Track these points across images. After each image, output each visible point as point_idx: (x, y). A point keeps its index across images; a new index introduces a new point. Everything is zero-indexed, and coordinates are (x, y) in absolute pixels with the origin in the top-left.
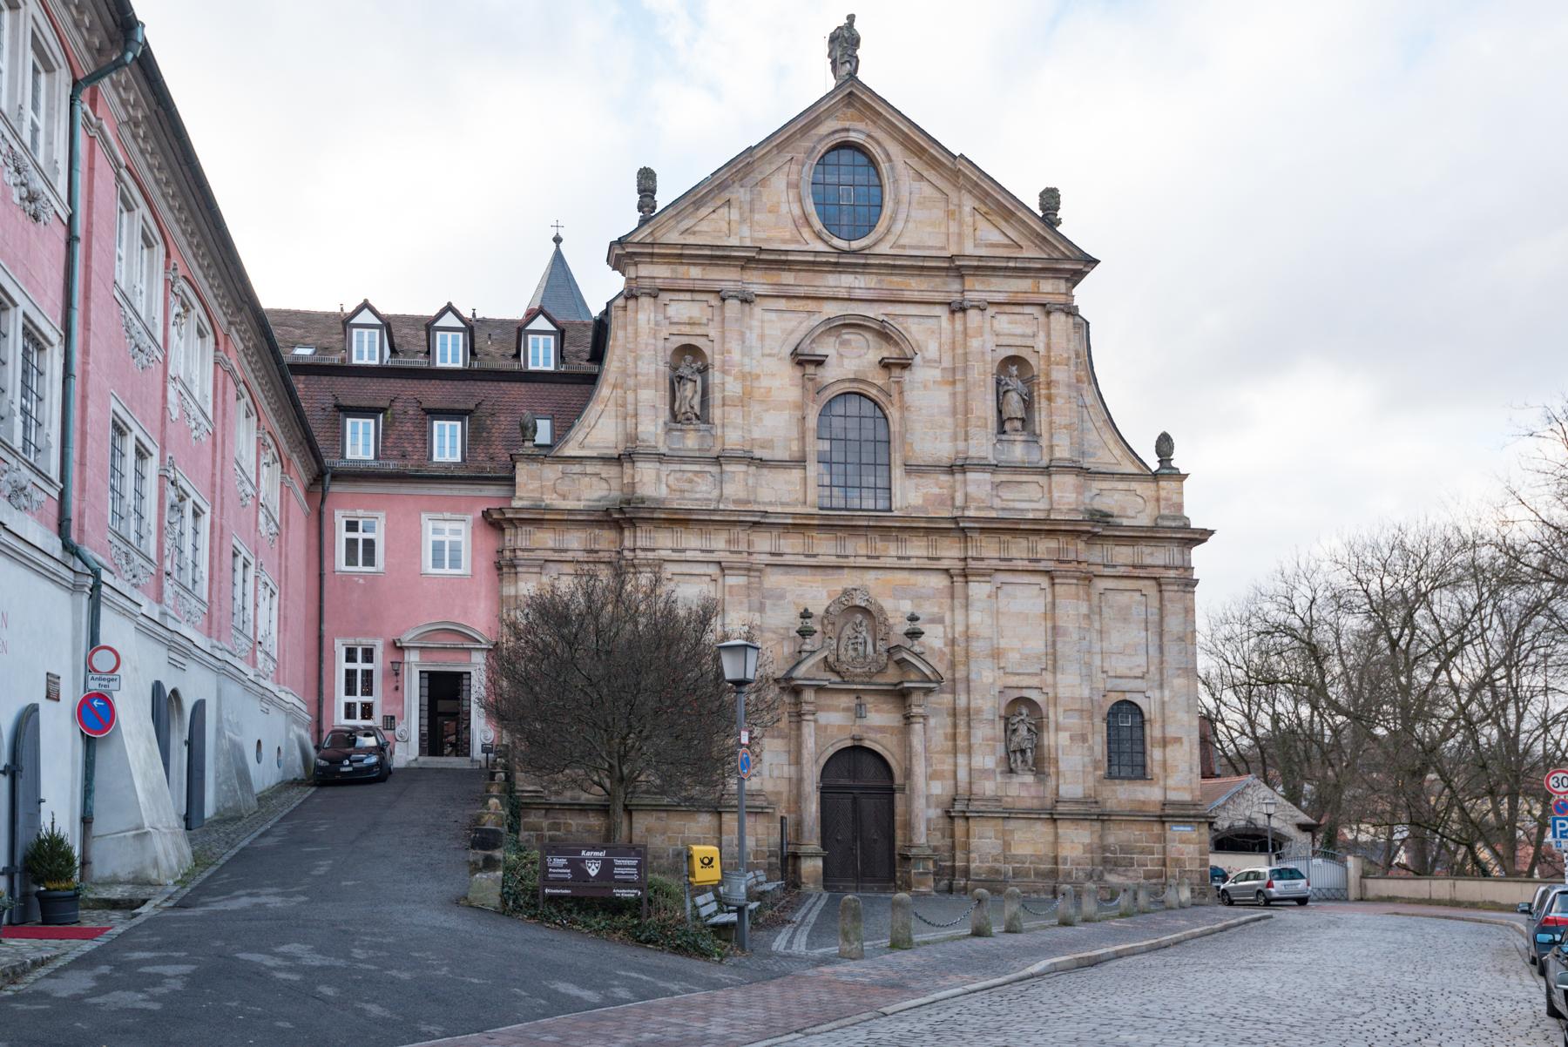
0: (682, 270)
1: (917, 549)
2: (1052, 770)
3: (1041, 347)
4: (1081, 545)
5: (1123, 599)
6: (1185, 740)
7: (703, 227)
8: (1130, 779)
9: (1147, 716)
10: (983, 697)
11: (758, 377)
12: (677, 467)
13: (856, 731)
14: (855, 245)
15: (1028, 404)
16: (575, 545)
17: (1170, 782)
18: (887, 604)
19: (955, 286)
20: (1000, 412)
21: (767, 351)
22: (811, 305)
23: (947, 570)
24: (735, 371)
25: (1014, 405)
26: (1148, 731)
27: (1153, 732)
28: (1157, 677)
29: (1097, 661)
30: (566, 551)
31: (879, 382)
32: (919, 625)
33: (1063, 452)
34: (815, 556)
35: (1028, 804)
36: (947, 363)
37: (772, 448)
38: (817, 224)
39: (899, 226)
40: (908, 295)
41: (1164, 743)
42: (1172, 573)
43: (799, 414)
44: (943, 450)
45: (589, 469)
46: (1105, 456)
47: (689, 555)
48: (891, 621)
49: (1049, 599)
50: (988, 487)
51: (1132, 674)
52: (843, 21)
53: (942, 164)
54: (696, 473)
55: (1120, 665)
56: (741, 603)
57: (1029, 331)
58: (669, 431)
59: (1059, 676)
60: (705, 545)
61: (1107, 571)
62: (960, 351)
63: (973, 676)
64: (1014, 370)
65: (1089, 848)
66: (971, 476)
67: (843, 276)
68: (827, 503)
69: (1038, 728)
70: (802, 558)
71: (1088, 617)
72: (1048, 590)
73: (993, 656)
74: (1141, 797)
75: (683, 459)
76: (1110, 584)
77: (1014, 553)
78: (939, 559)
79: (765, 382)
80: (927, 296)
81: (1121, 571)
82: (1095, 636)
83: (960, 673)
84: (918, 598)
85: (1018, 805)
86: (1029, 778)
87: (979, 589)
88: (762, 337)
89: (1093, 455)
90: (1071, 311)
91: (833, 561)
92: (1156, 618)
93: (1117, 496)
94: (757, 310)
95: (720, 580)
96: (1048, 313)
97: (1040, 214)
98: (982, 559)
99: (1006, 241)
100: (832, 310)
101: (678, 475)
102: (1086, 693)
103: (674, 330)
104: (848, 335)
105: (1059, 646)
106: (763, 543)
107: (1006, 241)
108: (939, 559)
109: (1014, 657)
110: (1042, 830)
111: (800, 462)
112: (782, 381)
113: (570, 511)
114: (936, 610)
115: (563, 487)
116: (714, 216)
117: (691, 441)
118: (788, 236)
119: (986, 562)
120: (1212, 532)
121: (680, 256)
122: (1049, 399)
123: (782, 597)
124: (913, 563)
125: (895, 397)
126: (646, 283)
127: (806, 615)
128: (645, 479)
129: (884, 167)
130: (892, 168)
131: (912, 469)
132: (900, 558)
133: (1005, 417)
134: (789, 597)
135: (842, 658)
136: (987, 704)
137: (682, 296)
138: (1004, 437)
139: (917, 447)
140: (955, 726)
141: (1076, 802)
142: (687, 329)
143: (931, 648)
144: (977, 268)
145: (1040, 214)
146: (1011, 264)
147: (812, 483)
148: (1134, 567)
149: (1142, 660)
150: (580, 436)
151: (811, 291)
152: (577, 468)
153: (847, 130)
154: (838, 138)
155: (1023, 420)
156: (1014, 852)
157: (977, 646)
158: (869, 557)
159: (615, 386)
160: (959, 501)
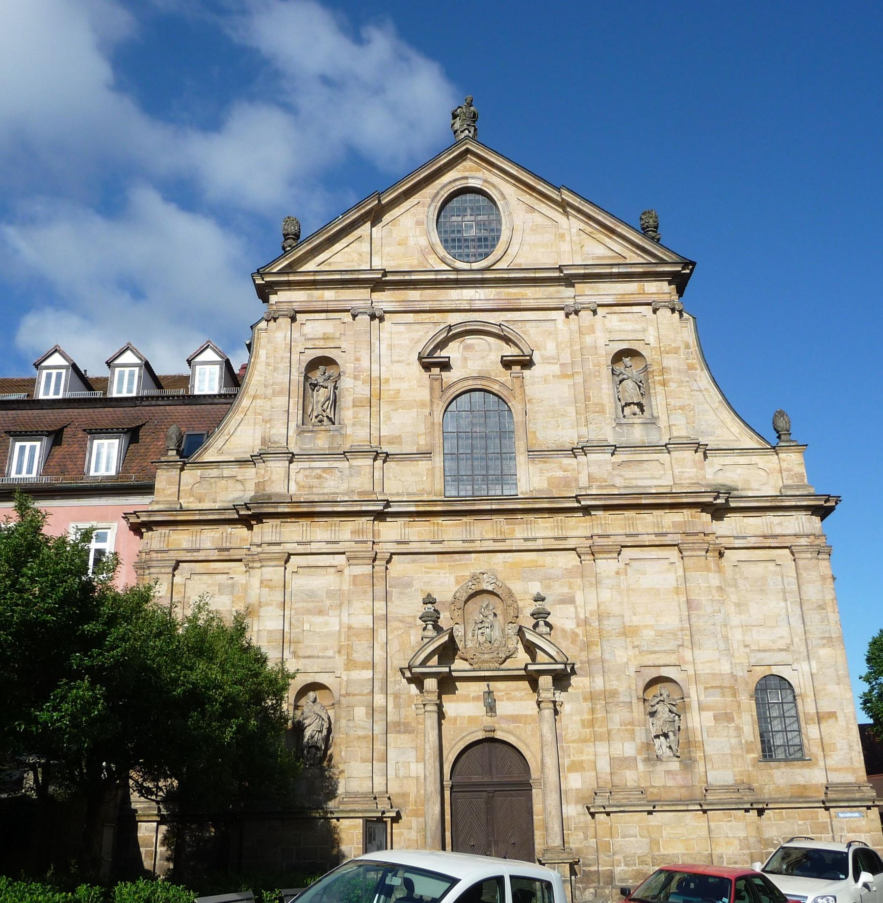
0: (317, 294)
1: (543, 529)
2: (699, 754)
3: (651, 339)
4: (706, 517)
5: (758, 570)
6: (840, 715)
7: (337, 258)
8: (786, 760)
9: (797, 691)
10: (618, 678)
11: (387, 380)
12: (306, 465)
13: (488, 721)
14: (475, 266)
16: (208, 545)
17: (830, 762)
18: (516, 587)
19: (569, 292)
21: (395, 358)
22: (436, 316)
23: (574, 549)
24: (365, 375)
25: (630, 391)
26: (800, 707)
27: (807, 707)
28: (803, 648)
29: (737, 636)
30: (198, 550)
31: (502, 380)
32: (547, 606)
33: (681, 431)
34: (441, 542)
35: (676, 794)
36: (566, 358)
37: (400, 443)
38: (442, 252)
39: (512, 251)
40: (524, 304)
41: (820, 718)
42: (804, 541)
43: (427, 411)
44: (569, 436)
45: (227, 471)
47: (314, 547)
48: (520, 604)
49: (681, 572)
50: (610, 467)
54: (325, 469)
55: (763, 638)
56: (365, 592)
57: (639, 327)
58: (300, 432)
59: (696, 651)
60: (327, 536)
62: (577, 347)
63: (606, 656)
65: (744, 843)
66: (592, 457)
67: (465, 291)
68: (454, 493)
69: (679, 709)
70: (428, 545)
71: (720, 589)
72: (679, 564)
73: (624, 634)
74: (801, 781)
75: (310, 456)
77: (641, 530)
78: (566, 538)
79: (394, 385)
81: (752, 542)
82: (732, 609)
83: (596, 652)
84: (547, 580)
85: (665, 796)
86: (675, 765)
87: (606, 566)
88: (391, 347)
89: (711, 434)
91: (459, 546)
92: (795, 587)
93: (739, 470)
95: (347, 571)
96: (655, 311)
98: (608, 536)
100: (454, 319)
101: (307, 472)
102: (726, 668)
104: (470, 340)
105: (693, 619)
106: (390, 530)
108: (566, 538)
109: (648, 634)
110: (693, 822)
111: (426, 454)
114: (566, 590)
115: (198, 490)
117: (322, 442)
118: (415, 262)
119: (612, 539)
120: (838, 500)
122: (664, 384)
123: (409, 585)
124: (540, 544)
125: (518, 391)
126: (285, 307)
127: (429, 600)
128: (274, 477)
130: (507, 204)
131: (536, 454)
134: (417, 585)
135: (470, 644)
136: (628, 686)
138: (624, 421)
139: (540, 435)
140: (593, 711)
141: (727, 788)
142: (321, 343)
143: (564, 631)
146: (615, 270)
147: (439, 474)
148: (765, 537)
149: (784, 631)
150: (219, 443)
151: (436, 306)
152: (215, 472)
153: (467, 178)
154: (459, 185)
155: (640, 405)
156: (663, 851)
157: (610, 625)
158: (495, 540)
159: (254, 397)
160: (583, 481)
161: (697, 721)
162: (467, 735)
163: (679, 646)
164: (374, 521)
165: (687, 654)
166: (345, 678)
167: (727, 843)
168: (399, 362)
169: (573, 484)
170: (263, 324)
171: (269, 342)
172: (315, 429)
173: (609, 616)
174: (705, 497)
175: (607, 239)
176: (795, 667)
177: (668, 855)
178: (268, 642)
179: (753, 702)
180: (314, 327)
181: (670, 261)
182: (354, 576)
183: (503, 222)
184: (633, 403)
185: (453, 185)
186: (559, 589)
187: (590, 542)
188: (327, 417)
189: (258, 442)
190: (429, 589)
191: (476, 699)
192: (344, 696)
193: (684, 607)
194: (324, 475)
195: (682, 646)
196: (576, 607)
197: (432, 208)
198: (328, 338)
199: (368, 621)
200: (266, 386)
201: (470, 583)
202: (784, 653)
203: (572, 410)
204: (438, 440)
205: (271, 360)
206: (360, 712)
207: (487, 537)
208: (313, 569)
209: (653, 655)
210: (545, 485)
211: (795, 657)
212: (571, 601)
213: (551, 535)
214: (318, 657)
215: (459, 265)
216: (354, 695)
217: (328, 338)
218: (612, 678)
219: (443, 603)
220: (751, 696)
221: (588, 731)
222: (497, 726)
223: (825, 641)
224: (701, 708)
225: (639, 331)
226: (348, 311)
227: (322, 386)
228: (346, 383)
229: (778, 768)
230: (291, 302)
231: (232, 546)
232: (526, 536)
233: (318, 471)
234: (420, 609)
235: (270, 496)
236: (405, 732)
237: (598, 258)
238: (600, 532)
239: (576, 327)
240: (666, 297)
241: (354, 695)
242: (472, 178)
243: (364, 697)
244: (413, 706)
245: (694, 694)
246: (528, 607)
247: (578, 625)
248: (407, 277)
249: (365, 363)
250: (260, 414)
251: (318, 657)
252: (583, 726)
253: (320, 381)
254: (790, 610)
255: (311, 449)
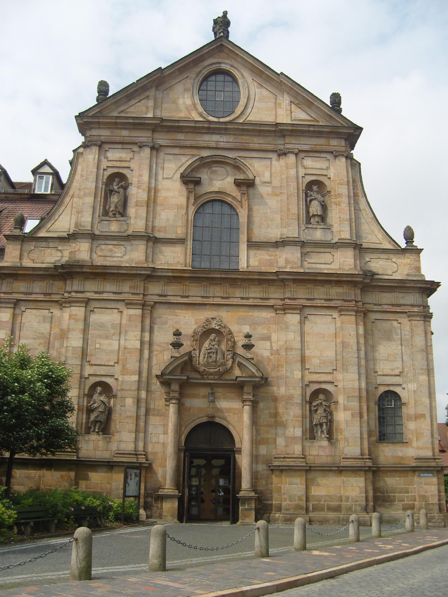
7: (132, 109)
9: (403, 401)
13: (210, 412)
14: (222, 120)
15: (324, 207)
18: (234, 328)
19: (281, 141)
20: (308, 212)
22: (194, 152)
23: (273, 306)
25: (315, 208)
27: (408, 411)
30: (31, 294)
31: (234, 194)
33: (346, 235)
37: (165, 232)
38: (201, 109)
40: (252, 146)
43: (184, 211)
44: (274, 233)
46: (371, 238)
47: (105, 296)
48: (236, 339)
49: (338, 324)
51: (393, 373)
52: (221, 15)
53: (273, 79)
56: (136, 326)
61: (376, 308)
62: (284, 177)
64: (315, 188)
74: (400, 454)
76: (379, 316)
80: (264, 147)
86: (325, 443)
87: (293, 319)
90: (350, 157)
91: (199, 300)
94: (162, 155)
97: (331, 106)
99: (309, 118)
100: (205, 153)
103: (110, 164)
105: (344, 354)
107: (309, 118)
108: (268, 299)
109: (316, 361)
112: (173, 192)
113: (34, 269)
114: (265, 331)
116: (138, 104)
117: (114, 227)
121: (115, 125)
124: (250, 302)
126: (96, 138)
127: (177, 334)
129: (240, 81)
131: (253, 245)
132: (242, 298)
133: (311, 214)
137: (116, 146)
138: (310, 226)
142: (118, 164)
144: (292, 131)
145: (331, 106)
146: (311, 129)
147: (189, 252)
148: (393, 305)
149: (398, 364)
151: (193, 143)
153: (220, 63)
154: (214, 67)
158: (222, 298)
159: (73, 197)
161: (341, 416)
162: (196, 419)
163: (333, 370)
164: (144, 280)
165: (339, 376)
166: (120, 379)
167: (352, 490)
168: (167, 178)
169: (275, 265)
170: (81, 150)
171: (84, 161)
172: (110, 219)
173: (291, 349)
174: (358, 277)
175: (308, 109)
176: (403, 386)
177: (316, 496)
178: (73, 354)
179: (377, 407)
180: (114, 154)
181: (346, 126)
182: (130, 315)
183: (242, 93)
184: (317, 215)
185: (211, 67)
186: (261, 331)
187: (283, 302)
188: (119, 212)
189: (73, 226)
190: (178, 327)
191: (204, 397)
192: (120, 390)
193: (339, 346)
194: (114, 249)
195: (336, 370)
196: (271, 343)
197: (196, 81)
198: (122, 161)
199: (137, 344)
200: (80, 190)
201: (205, 324)
202: (398, 377)
203: (278, 217)
204: (190, 231)
205: (84, 173)
206: (129, 402)
207: (217, 295)
208: (104, 310)
209: (317, 375)
210: (257, 264)
211: (404, 380)
212: (268, 338)
213: (259, 296)
214: (104, 365)
215: (211, 119)
216: (126, 390)
217: (122, 161)
218: (290, 388)
219: (186, 335)
220: (376, 403)
221: (273, 420)
222: (216, 414)
223: (423, 371)
224: (345, 409)
225: (324, 169)
226: (136, 143)
227: (116, 192)
228: (133, 191)
229: (387, 446)
230: (100, 136)
231: (53, 292)
232: (242, 296)
233: (111, 246)
234: (172, 339)
235: (78, 261)
236: (157, 415)
237: (301, 120)
238: (290, 296)
239: (284, 164)
240: (343, 149)
241: (126, 390)
242: (224, 63)
243: (132, 392)
244: (164, 400)
245: (341, 399)
246: (241, 341)
247: (272, 354)
248: (176, 124)
249: (146, 178)
250: (75, 208)
251: (104, 365)
252: (270, 417)
253: (116, 188)
254: (404, 351)
255: (106, 232)
